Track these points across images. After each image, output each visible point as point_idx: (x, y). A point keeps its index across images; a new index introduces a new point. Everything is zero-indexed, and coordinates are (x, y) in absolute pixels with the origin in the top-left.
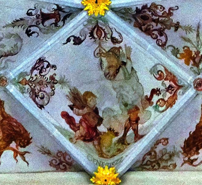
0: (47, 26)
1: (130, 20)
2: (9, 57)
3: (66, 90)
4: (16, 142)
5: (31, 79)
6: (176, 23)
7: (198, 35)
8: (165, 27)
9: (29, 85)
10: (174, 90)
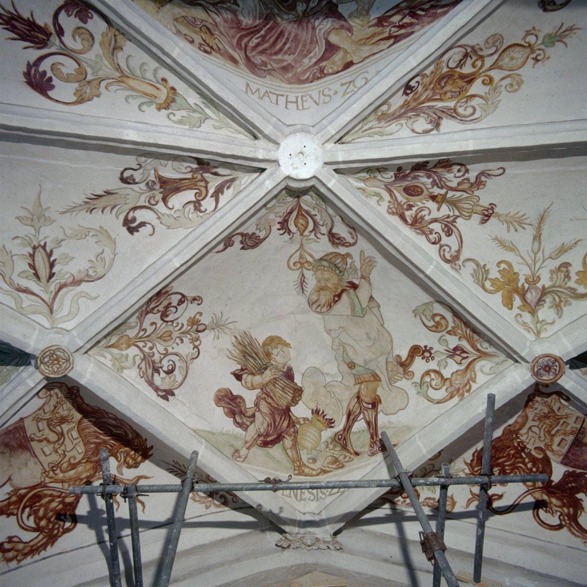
1: (377, 194)
2: (84, 287)
3: (227, 342)
4: (117, 458)
6: (487, 205)
7: (537, 237)
8: (457, 213)
9: (138, 347)
10: (467, 357)
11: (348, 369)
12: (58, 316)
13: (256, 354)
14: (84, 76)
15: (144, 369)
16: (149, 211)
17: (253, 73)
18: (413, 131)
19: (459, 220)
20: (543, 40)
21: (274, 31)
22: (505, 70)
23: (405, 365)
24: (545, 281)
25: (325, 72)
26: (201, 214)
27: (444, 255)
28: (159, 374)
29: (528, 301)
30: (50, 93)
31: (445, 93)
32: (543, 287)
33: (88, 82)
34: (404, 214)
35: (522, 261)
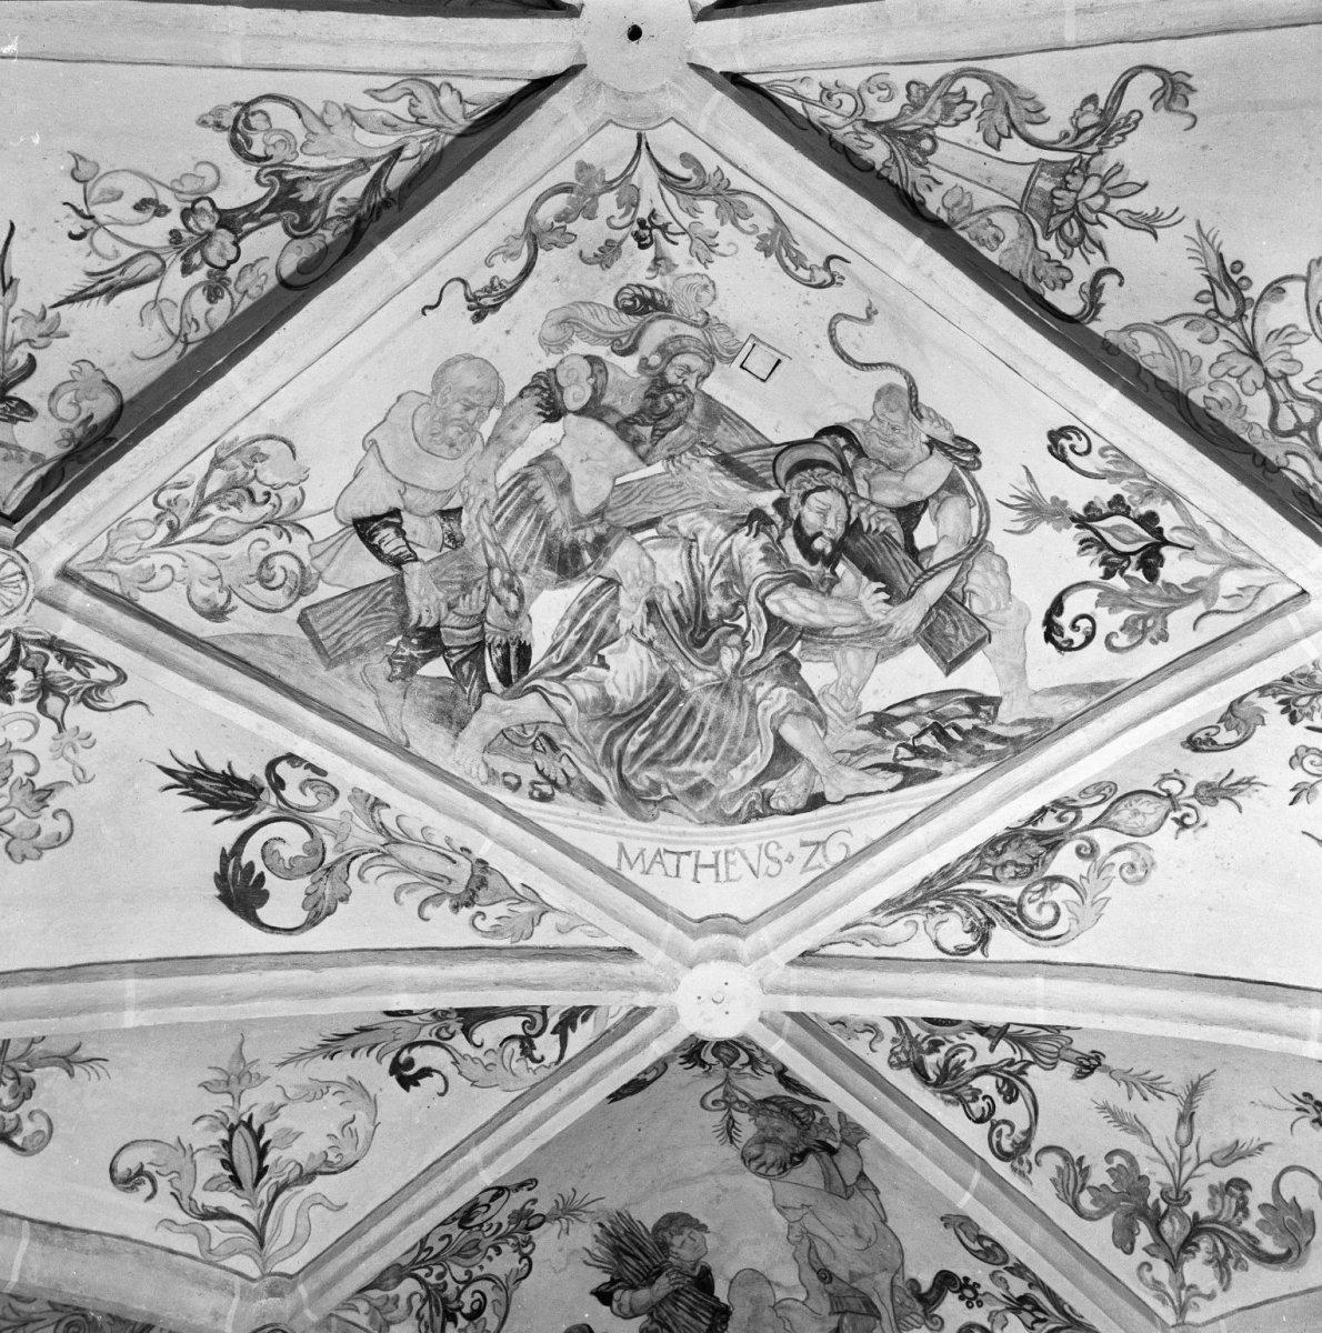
0: (487, 1045)
3: (584, 1235)
5: (424, 1255)
7: (1187, 1118)
8: (1028, 1056)
9: (416, 1277)
11: (818, 1282)
12: (274, 1249)
13: (641, 1249)
14: (320, 855)
15: (427, 1317)
16: (437, 1049)
17: (632, 815)
18: (936, 943)
19: (1033, 1070)
20: (1196, 790)
21: (676, 711)
22: (1122, 832)
23: (928, 1300)
24: (1199, 1205)
25: (773, 805)
26: (534, 1066)
27: (999, 1144)
28: (456, 1323)
29: (1167, 1238)
30: (261, 913)
31: (1004, 866)
32: (1196, 1215)
33: (328, 869)
34: (921, 1061)
35: (1156, 1155)
